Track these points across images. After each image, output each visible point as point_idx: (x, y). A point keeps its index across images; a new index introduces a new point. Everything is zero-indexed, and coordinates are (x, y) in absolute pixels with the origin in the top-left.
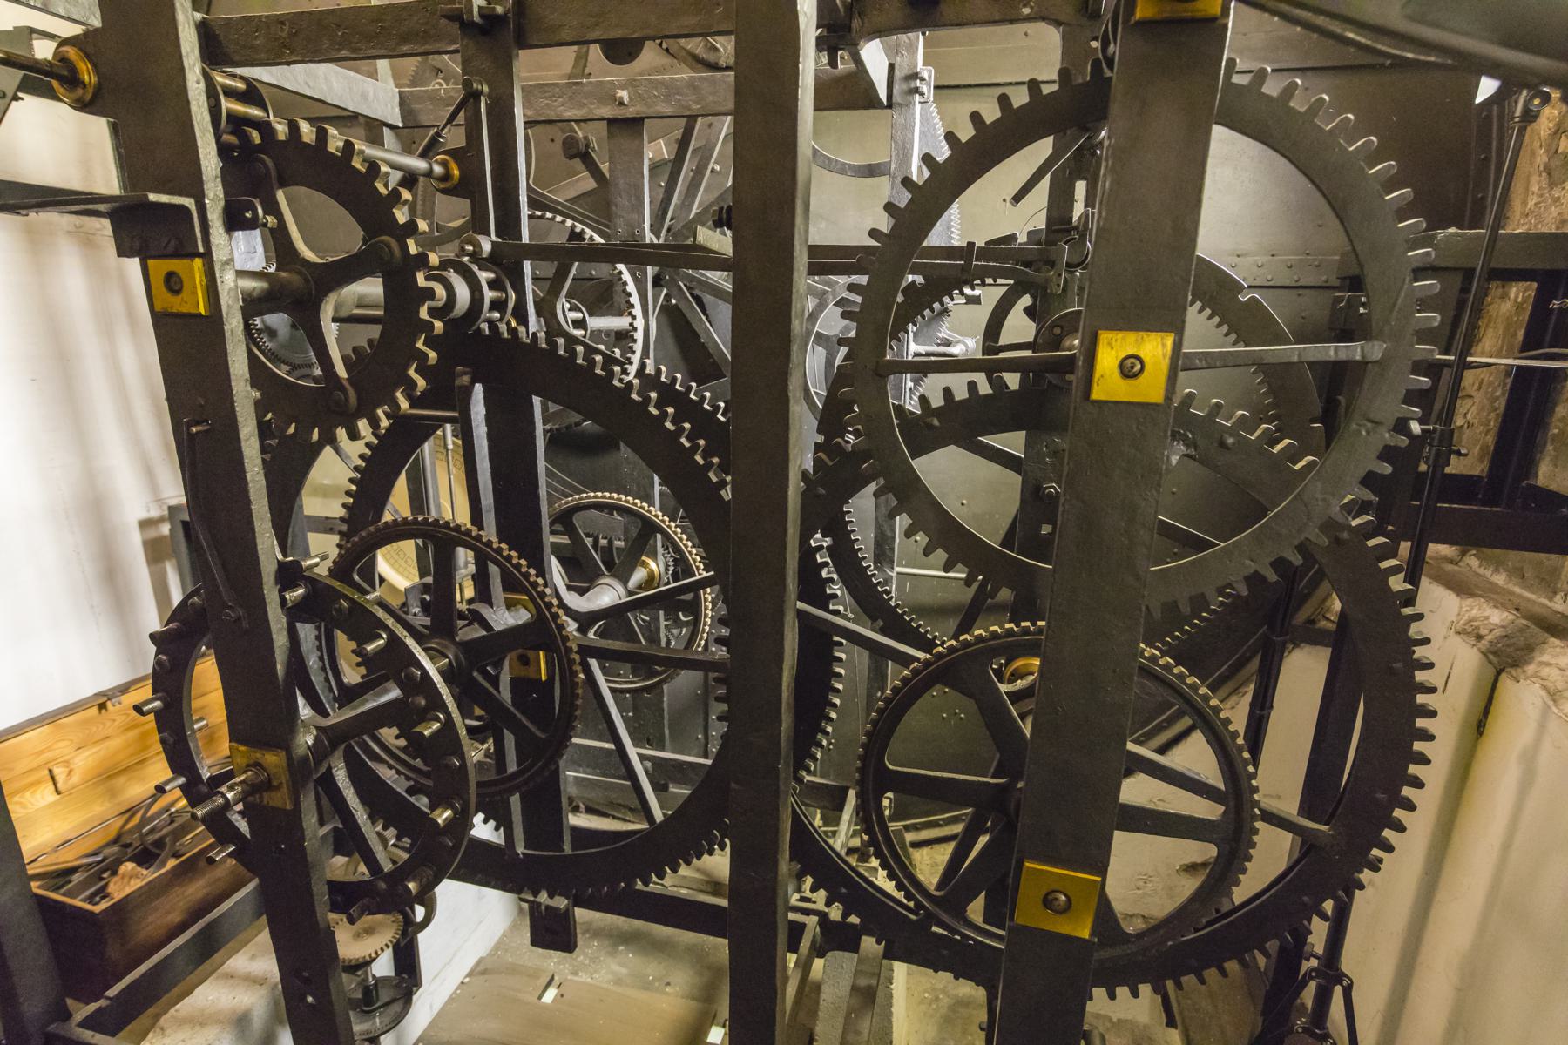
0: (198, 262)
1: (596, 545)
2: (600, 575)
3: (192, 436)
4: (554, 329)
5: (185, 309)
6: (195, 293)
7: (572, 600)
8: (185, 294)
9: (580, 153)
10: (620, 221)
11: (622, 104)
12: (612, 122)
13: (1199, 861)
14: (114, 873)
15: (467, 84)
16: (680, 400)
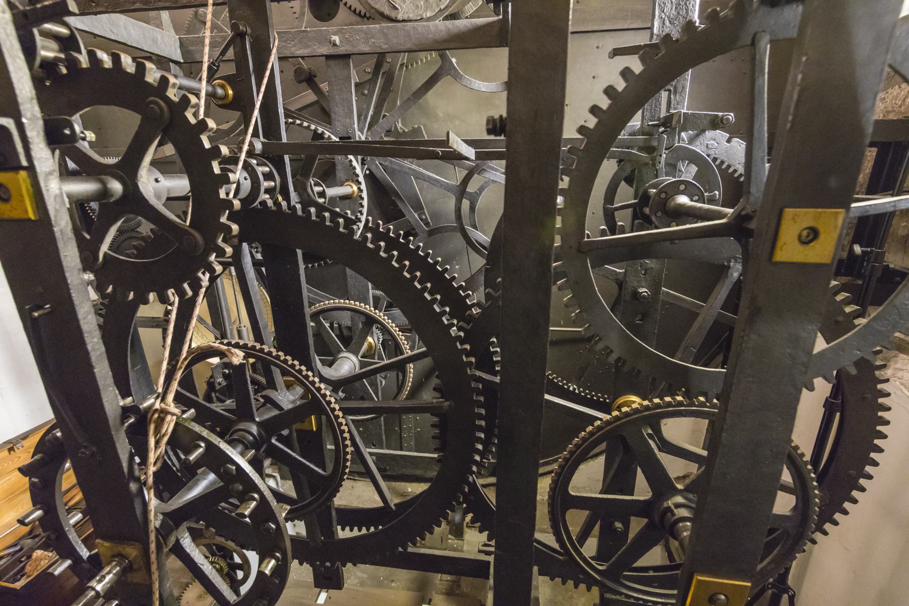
0: (23, 174)
1: (332, 327)
2: (340, 351)
3: (35, 321)
4: (307, 202)
5: (16, 214)
6: (23, 201)
7: (327, 372)
8: (13, 202)
9: (309, 80)
10: (337, 124)
11: (335, 45)
12: (329, 57)
13: (681, 475)
14: (29, 557)
15: (234, 27)
16: (385, 236)
